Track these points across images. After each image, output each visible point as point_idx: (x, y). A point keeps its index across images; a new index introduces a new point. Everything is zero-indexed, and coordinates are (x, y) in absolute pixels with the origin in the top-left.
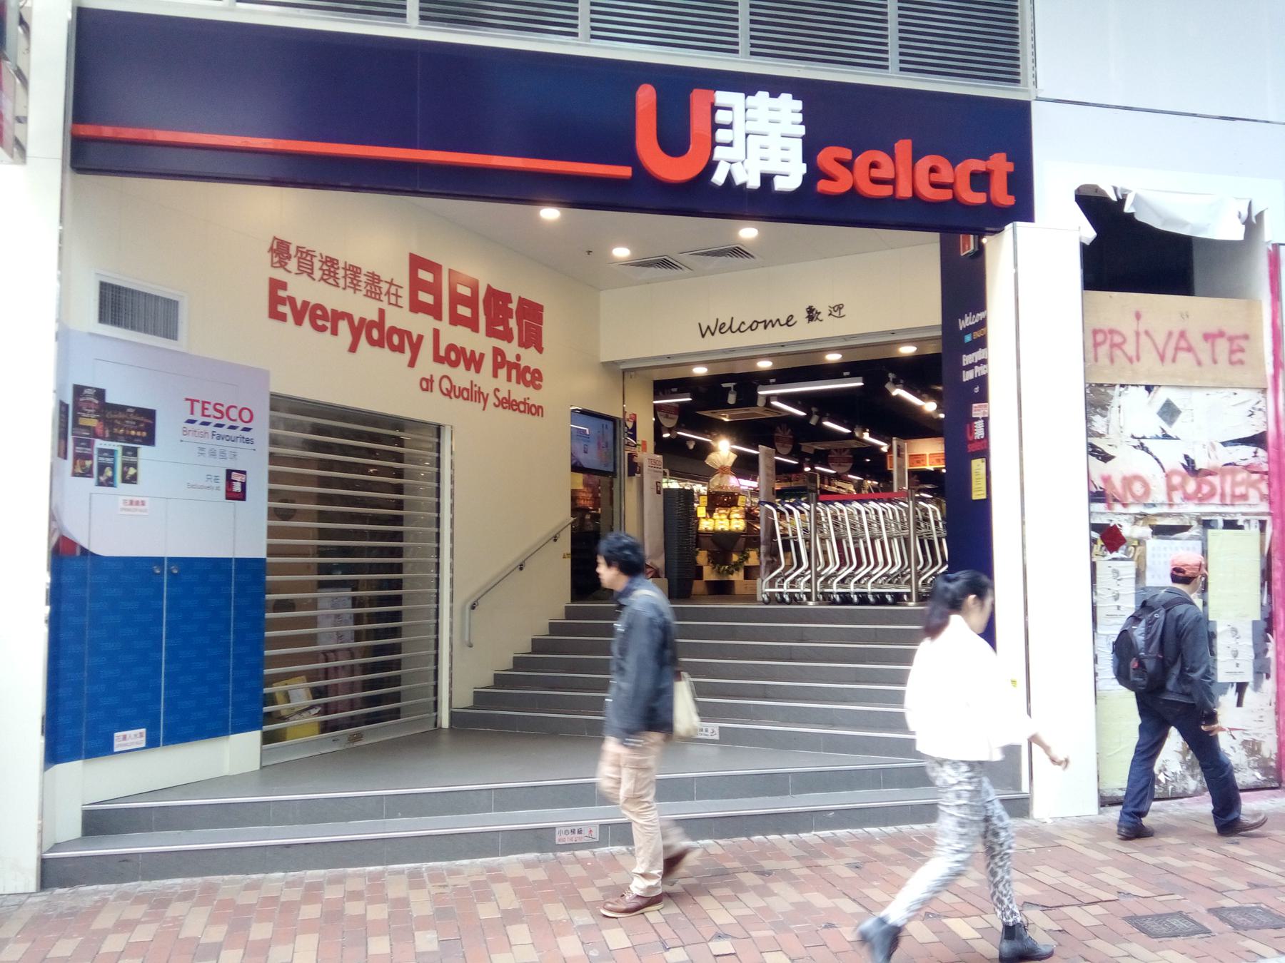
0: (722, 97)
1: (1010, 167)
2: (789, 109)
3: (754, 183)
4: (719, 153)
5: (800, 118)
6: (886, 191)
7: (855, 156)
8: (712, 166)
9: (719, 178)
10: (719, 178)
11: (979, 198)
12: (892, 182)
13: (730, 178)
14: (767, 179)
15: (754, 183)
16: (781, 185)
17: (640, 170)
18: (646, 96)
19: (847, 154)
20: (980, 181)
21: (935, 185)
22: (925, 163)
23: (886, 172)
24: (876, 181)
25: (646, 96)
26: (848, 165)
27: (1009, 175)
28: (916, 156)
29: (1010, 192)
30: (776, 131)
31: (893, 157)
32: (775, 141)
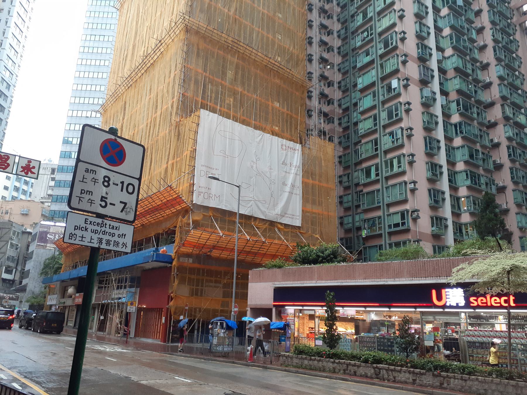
1: (514, 298)
5: (463, 292)
6: (485, 305)
7: (477, 299)
8: (446, 302)
11: (506, 305)
12: (486, 303)
13: (450, 305)
14: (457, 304)
19: (475, 298)
21: (496, 303)
22: (493, 299)
23: (485, 301)
24: (482, 303)
26: (476, 300)
27: (513, 300)
28: (491, 298)
29: (514, 303)
31: (486, 298)
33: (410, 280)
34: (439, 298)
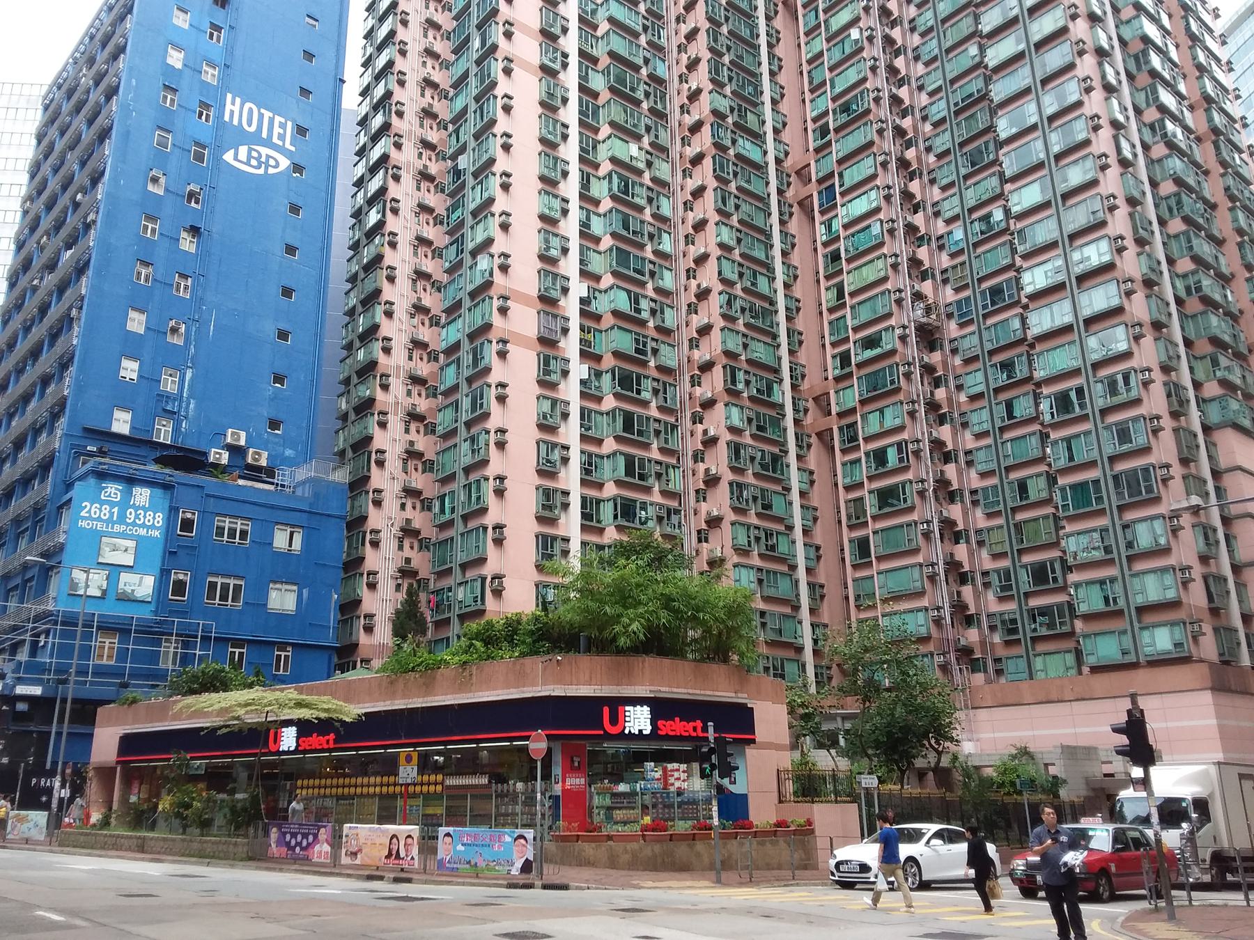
0: (627, 708)
2: (646, 709)
3: (637, 733)
4: (627, 724)
8: (625, 728)
9: (627, 731)
10: (627, 731)
14: (640, 731)
15: (637, 733)
16: (645, 732)
17: (605, 731)
18: (606, 710)
20: (695, 729)
25: (606, 710)
30: (642, 717)
32: (642, 720)
33: (560, 681)
34: (615, 720)
